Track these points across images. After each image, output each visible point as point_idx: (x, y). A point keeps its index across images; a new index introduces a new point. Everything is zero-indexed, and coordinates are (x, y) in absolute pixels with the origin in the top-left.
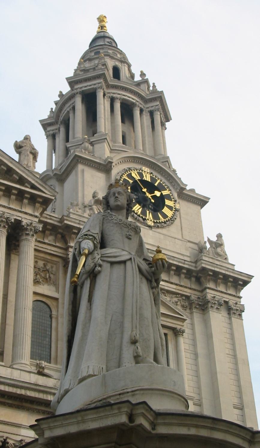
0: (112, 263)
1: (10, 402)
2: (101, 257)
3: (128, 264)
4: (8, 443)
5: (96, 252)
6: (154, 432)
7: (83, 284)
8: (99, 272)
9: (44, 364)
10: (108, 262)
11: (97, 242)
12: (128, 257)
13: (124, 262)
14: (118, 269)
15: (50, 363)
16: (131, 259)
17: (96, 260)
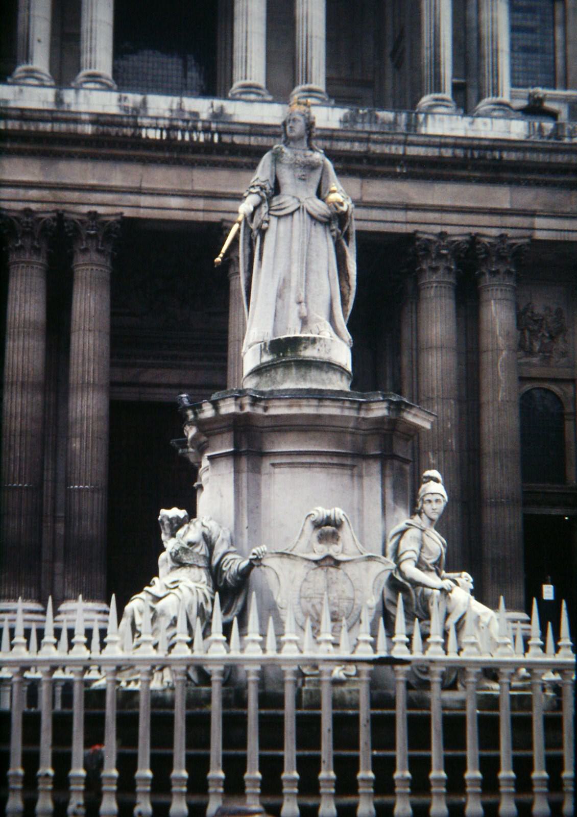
0: (279, 217)
1: (477, 174)
2: (269, 210)
3: (296, 215)
4: (479, 243)
5: (263, 205)
6: (267, 414)
7: (256, 239)
8: (267, 229)
9: (541, 91)
10: (276, 216)
11: (266, 194)
12: (296, 207)
13: (292, 214)
14: (284, 225)
15: (554, 87)
16: (298, 209)
17: (263, 215)
